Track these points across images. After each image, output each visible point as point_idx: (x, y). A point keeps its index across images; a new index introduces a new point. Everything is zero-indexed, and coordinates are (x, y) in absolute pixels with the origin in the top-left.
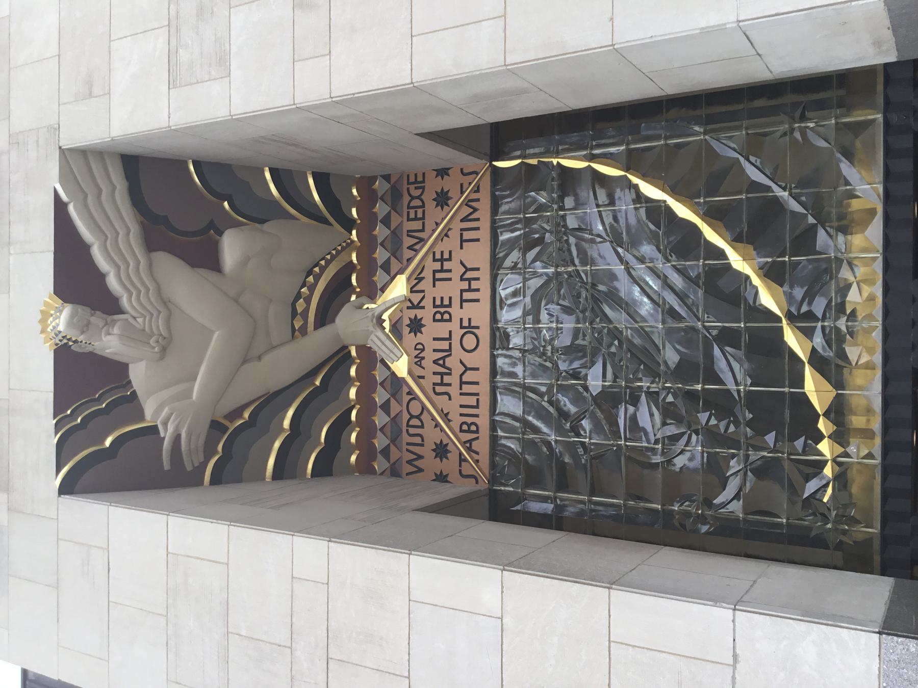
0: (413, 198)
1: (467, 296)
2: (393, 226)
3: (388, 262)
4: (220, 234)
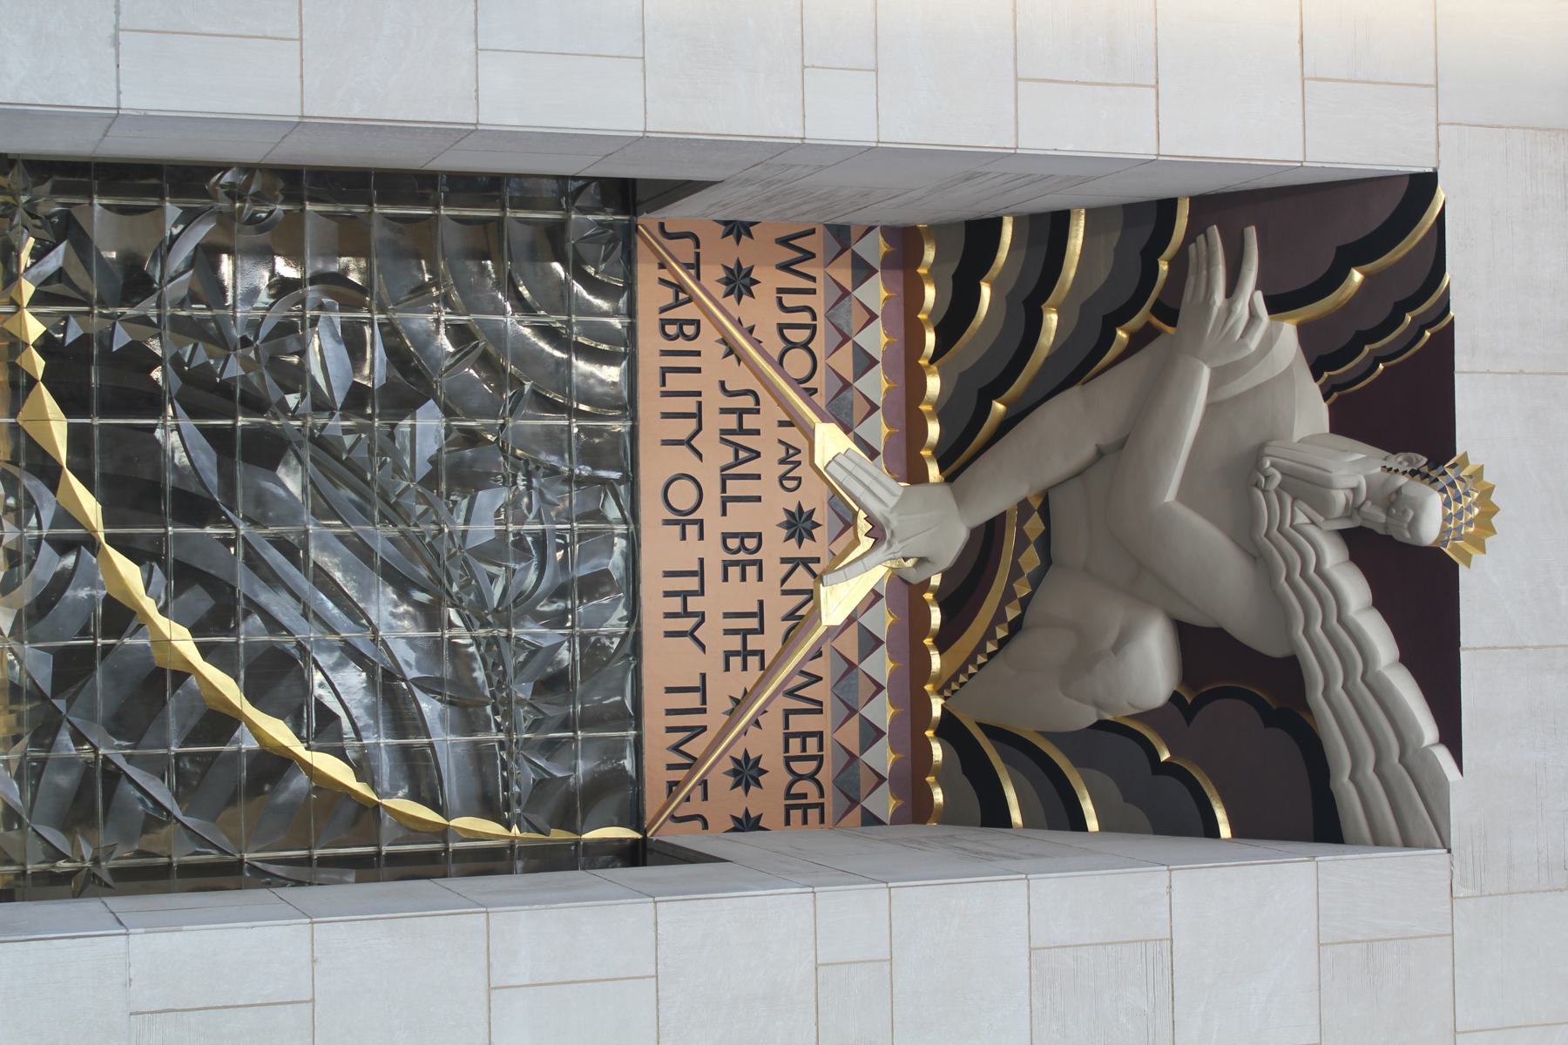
0: (812, 777)
1: (692, 584)
2: (854, 722)
3: (865, 653)
4: (1175, 698)
